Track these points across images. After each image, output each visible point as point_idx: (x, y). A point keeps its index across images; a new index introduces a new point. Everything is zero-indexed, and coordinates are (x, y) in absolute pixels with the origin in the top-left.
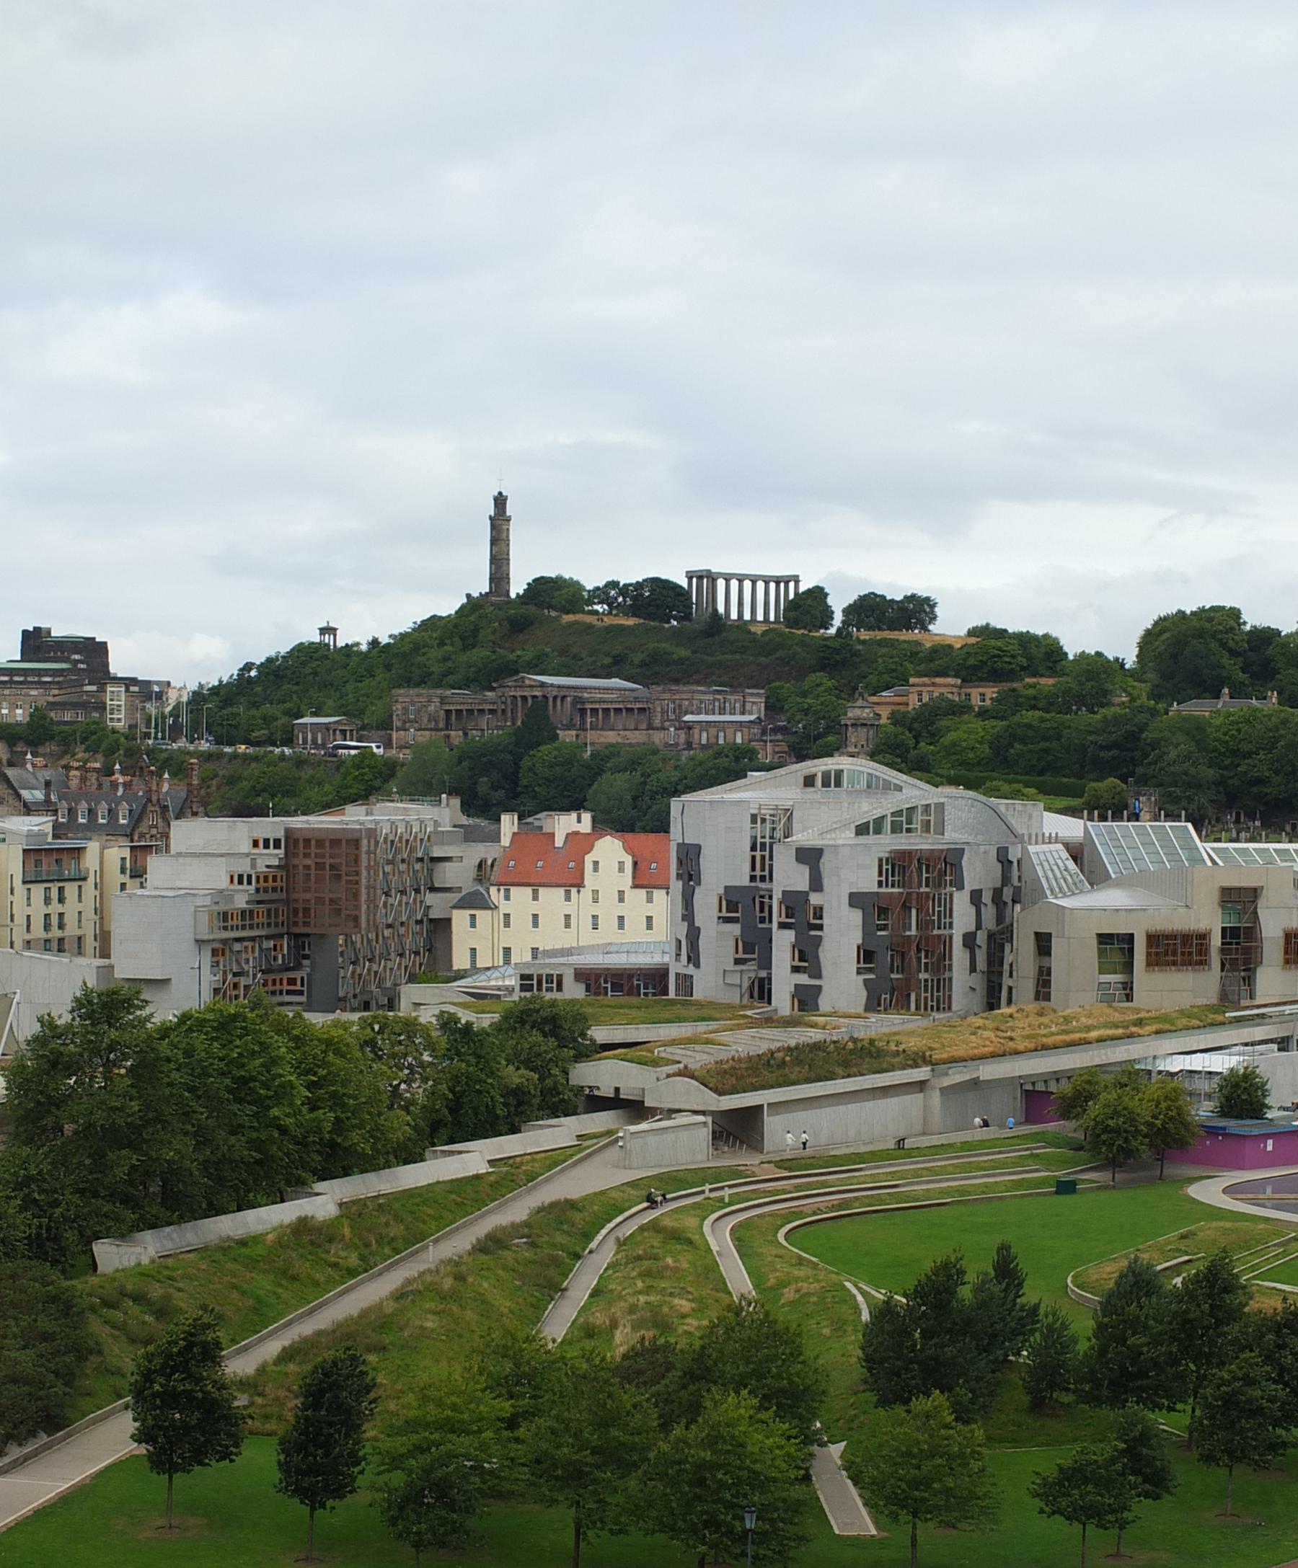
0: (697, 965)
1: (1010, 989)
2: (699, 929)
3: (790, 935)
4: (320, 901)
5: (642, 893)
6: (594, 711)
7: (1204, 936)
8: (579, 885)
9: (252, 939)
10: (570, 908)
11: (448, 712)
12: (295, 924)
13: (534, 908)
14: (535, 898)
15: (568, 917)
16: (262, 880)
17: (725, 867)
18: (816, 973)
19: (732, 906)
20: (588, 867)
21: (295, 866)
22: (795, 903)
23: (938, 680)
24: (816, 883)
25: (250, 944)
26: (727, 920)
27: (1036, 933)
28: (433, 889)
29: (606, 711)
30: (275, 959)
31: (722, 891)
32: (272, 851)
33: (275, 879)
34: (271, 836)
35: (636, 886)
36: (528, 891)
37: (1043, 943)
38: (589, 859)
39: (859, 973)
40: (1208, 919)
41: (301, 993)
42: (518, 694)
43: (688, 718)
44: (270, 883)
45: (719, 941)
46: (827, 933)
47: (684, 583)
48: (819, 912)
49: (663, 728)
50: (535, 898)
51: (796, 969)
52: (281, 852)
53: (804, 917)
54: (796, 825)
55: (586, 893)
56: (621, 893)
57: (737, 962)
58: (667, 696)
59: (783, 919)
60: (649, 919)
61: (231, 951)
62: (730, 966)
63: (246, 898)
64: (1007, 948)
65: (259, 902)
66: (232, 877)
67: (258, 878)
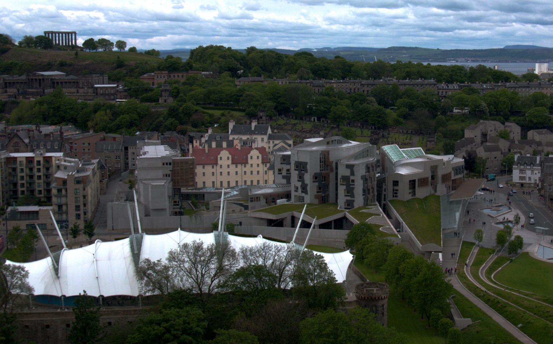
0: (306, 193)
1: (385, 195)
2: (307, 185)
5: (234, 165)
6: (58, 83)
7: (427, 178)
8: (216, 164)
10: (214, 170)
11: (6, 83)
13: (204, 171)
14: (204, 168)
15: (213, 173)
17: (314, 168)
18: (353, 196)
19: (316, 178)
20: (219, 159)
23: (163, 72)
24: (352, 173)
27: (394, 181)
29: (62, 83)
31: (313, 174)
32: (169, 166)
34: (168, 162)
35: (233, 163)
36: (202, 166)
37: (396, 183)
38: (219, 157)
39: (363, 195)
40: (429, 175)
41: (178, 205)
42: (34, 78)
43: (96, 86)
45: (312, 187)
47: (44, 35)
48: (353, 181)
49: (83, 88)
50: (204, 168)
51: (346, 196)
53: (348, 182)
54: (330, 156)
55: (219, 166)
56: (228, 166)
57: (317, 192)
58: (83, 78)
59: (342, 183)
60: (237, 172)
62: (316, 194)
64: (384, 184)
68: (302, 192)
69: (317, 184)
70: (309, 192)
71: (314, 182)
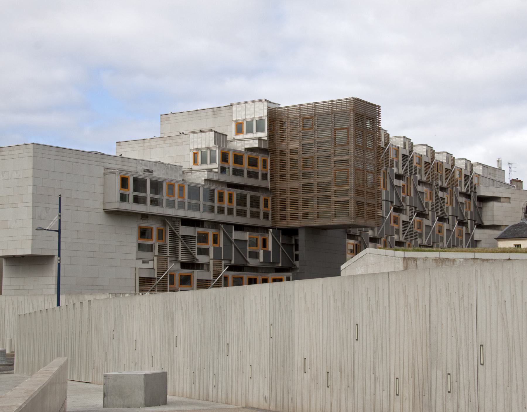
4: (307, 187)
9: (215, 225)
12: (283, 217)
16: (231, 159)
21: (283, 153)
25: (211, 233)
28: (481, 226)
30: (255, 255)
33: (253, 162)
44: (246, 166)
52: (264, 135)
61: (173, 235)
63: (205, 175)
65: (230, 185)
66: (195, 155)
67: (224, 157)
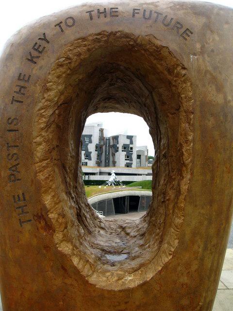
0: (90, 159)
2: (91, 152)
3: (125, 153)
18: (131, 160)
22: (125, 147)
24: (132, 143)
26: (96, 151)
46: (133, 152)
48: (132, 148)
51: (126, 160)
68: (85, 159)
69: (97, 152)
70: (92, 159)
71: (96, 151)
